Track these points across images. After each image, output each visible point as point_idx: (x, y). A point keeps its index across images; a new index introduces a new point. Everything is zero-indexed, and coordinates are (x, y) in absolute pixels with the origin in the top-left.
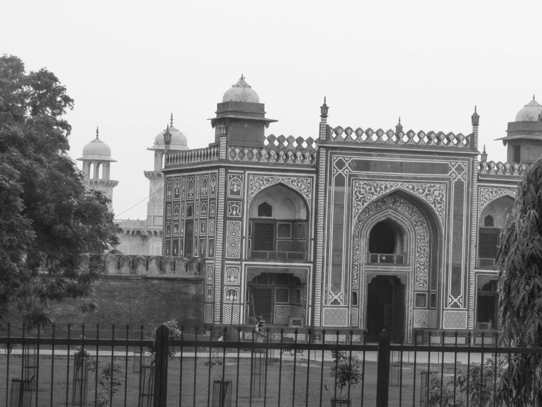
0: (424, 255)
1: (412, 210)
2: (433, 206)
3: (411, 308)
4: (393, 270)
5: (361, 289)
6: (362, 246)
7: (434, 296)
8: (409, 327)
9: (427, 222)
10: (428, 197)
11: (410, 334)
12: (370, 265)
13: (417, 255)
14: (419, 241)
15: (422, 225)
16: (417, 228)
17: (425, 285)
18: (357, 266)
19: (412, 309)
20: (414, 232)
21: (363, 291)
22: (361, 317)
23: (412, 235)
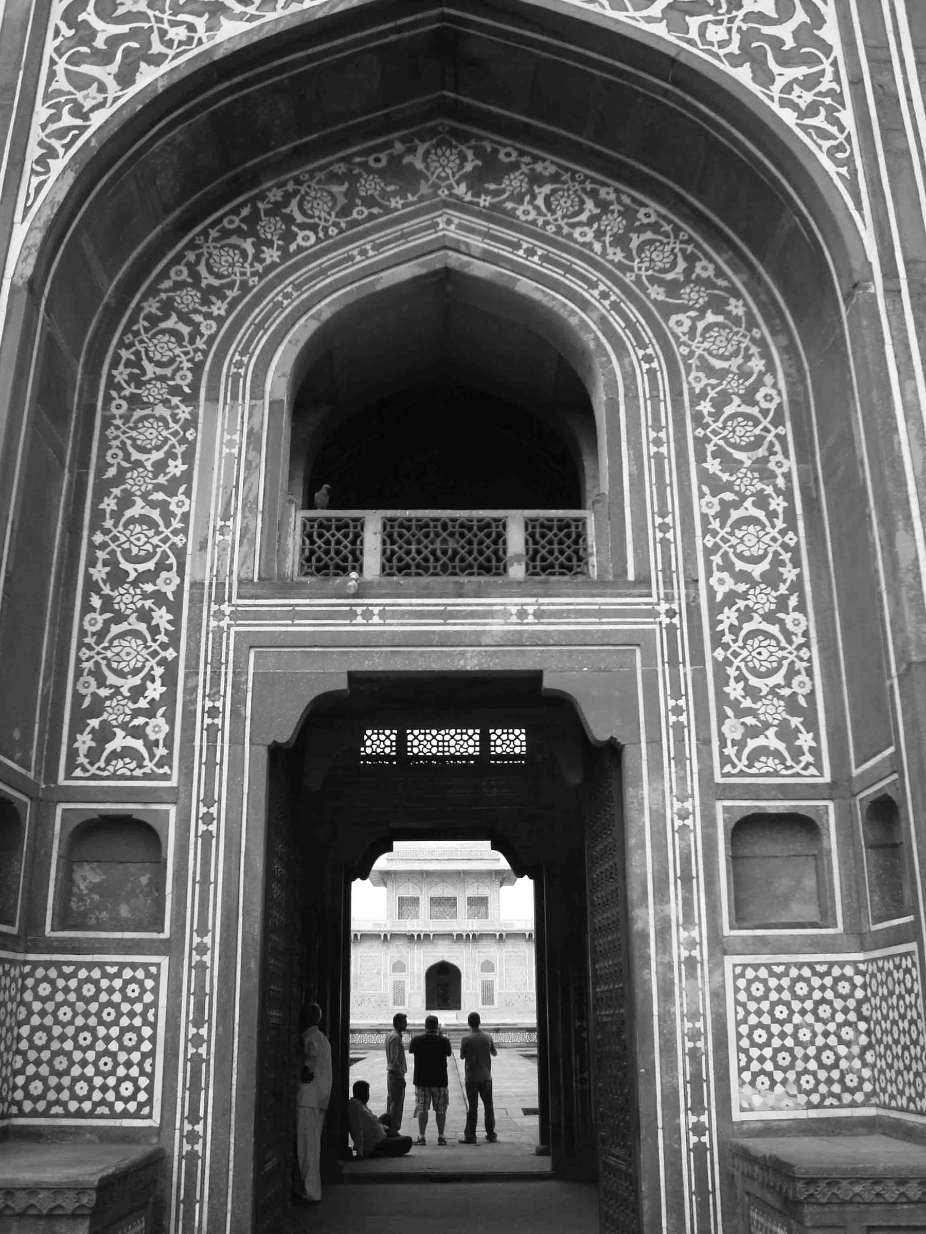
0: (762, 501)
1: (628, 214)
2: (743, 74)
3: (687, 940)
4: (496, 626)
5: (197, 790)
6: (220, 451)
7: (885, 811)
8: (686, 1120)
9: (754, 282)
10: (694, 23)
11: (702, 1190)
12: (284, 588)
13: (705, 504)
14: (705, 407)
15: (717, 305)
16: (679, 324)
17: (805, 740)
18: (175, 608)
19: (702, 953)
20: (654, 349)
21: (220, 810)
22: (201, 1039)
23: (640, 370)
